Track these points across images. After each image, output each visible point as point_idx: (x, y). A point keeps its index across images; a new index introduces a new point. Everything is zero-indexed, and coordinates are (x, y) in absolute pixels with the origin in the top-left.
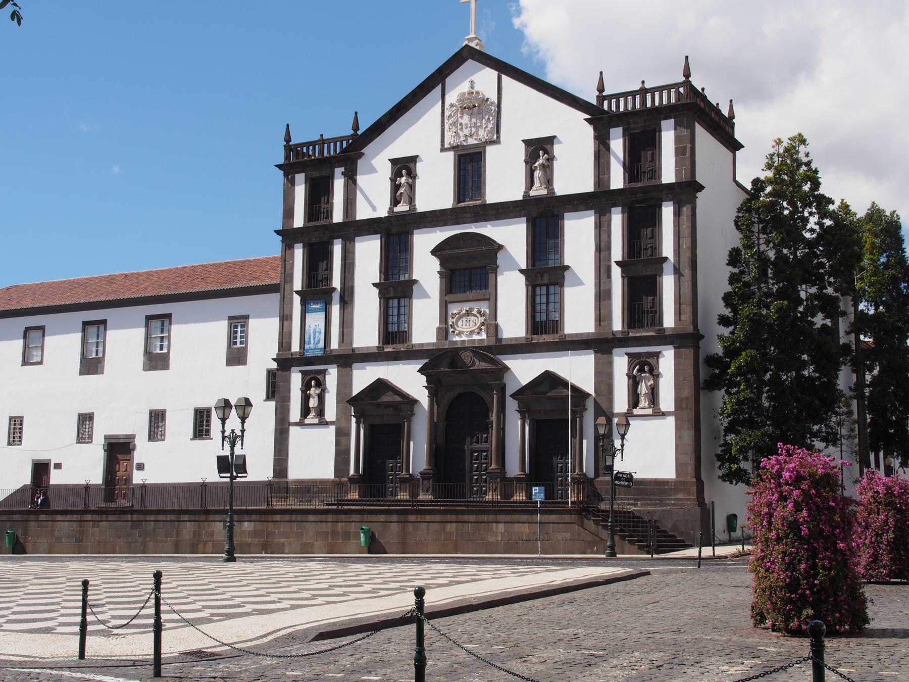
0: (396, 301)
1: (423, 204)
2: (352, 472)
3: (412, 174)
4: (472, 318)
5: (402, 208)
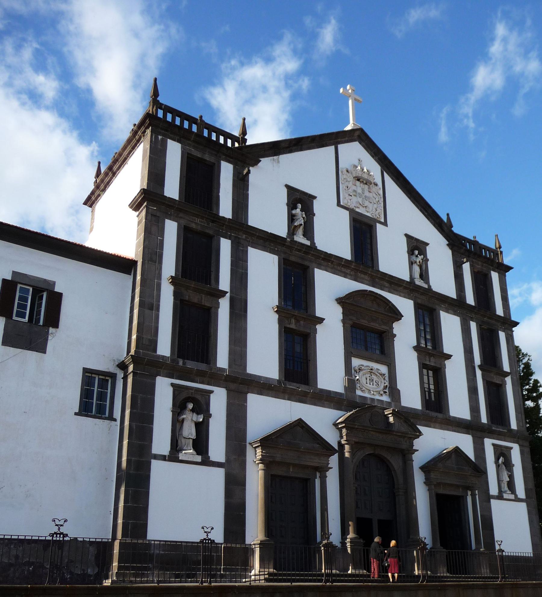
4: (374, 377)
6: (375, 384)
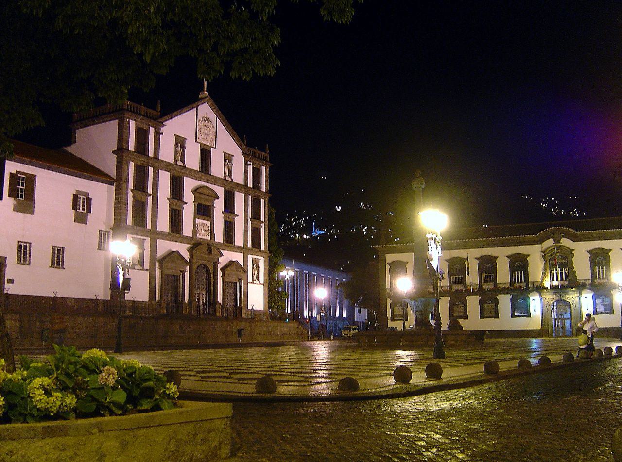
3: (183, 147)
5: (180, 163)
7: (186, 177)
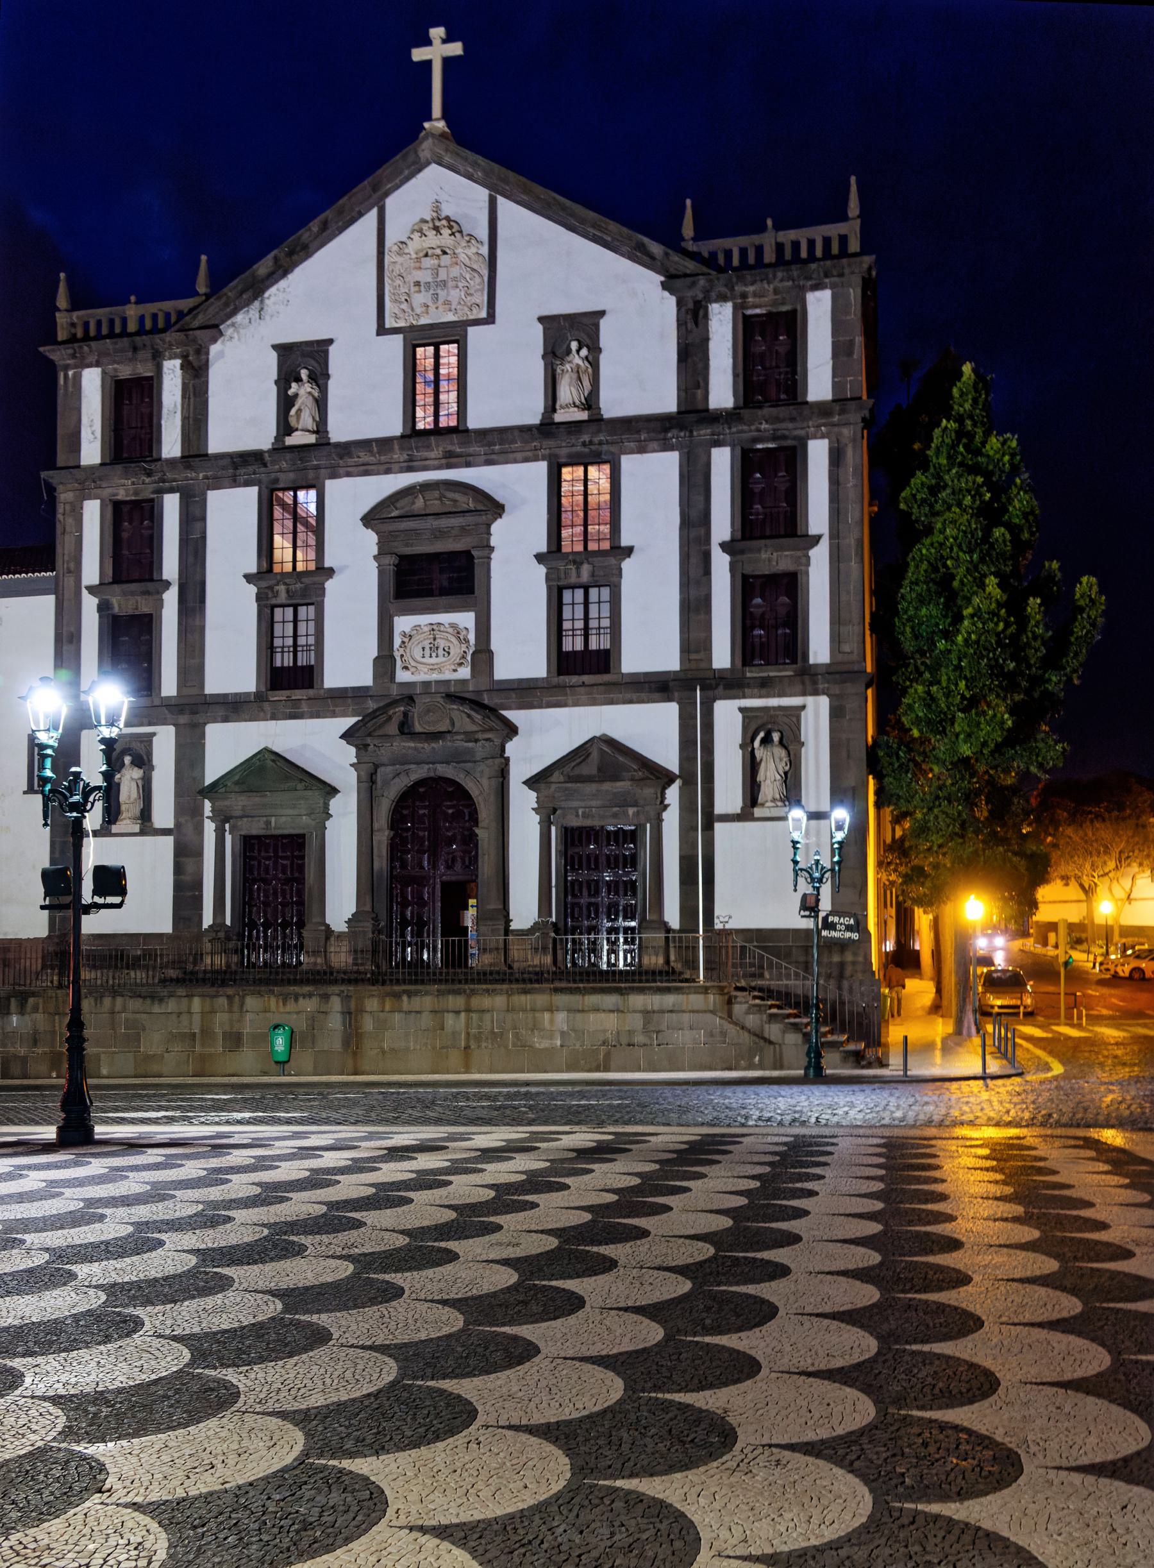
0: (290, 611)
1: (340, 430)
2: (208, 920)
3: (320, 378)
6: (441, 652)
7: (334, 476)
